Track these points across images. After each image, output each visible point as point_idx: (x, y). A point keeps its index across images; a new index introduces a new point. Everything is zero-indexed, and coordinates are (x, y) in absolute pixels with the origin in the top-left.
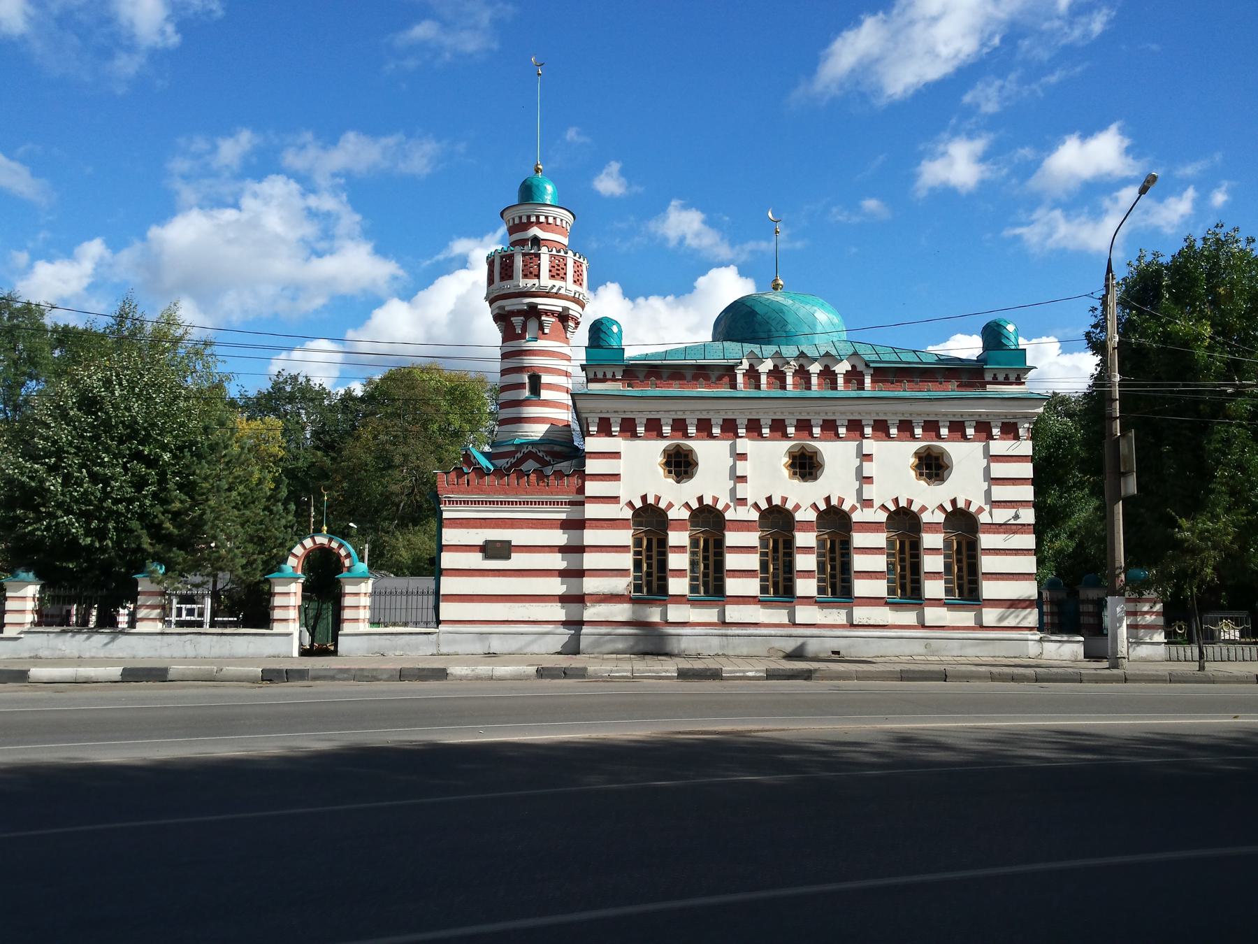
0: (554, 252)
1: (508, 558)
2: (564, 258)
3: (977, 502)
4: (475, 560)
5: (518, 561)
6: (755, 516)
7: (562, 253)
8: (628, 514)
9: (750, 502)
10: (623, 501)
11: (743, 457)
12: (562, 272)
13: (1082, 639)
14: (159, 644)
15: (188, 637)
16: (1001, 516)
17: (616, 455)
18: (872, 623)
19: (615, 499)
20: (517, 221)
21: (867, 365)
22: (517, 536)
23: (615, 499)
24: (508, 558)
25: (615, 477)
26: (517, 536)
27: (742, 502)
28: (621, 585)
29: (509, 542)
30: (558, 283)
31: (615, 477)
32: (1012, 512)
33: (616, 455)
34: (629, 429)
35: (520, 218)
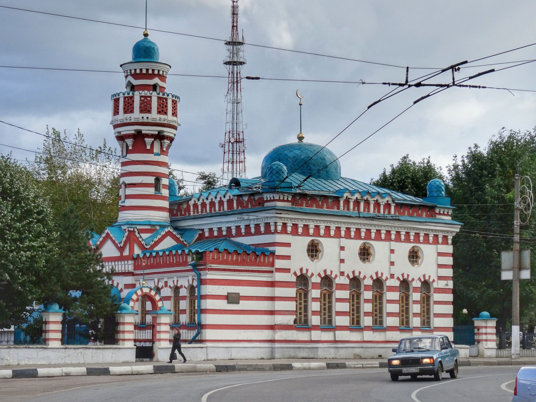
0: (161, 95)
1: (238, 303)
2: (166, 99)
3: (434, 277)
4: (223, 304)
5: (244, 305)
6: (347, 282)
7: (165, 96)
8: (294, 279)
9: (346, 274)
10: (292, 271)
11: (342, 248)
12: (164, 109)
13: (469, 347)
14: (64, 355)
15: (80, 350)
16: (442, 284)
17: (288, 245)
18: (393, 340)
19: (288, 270)
20: (138, 71)
21: (393, 201)
22: (243, 291)
23: (288, 270)
24: (238, 303)
25: (288, 257)
26: (243, 291)
27: (342, 274)
28: (290, 320)
29: (239, 294)
30: (163, 117)
31: (288, 257)
32: (445, 282)
33: (288, 245)
34: (295, 232)
35: (135, 70)
